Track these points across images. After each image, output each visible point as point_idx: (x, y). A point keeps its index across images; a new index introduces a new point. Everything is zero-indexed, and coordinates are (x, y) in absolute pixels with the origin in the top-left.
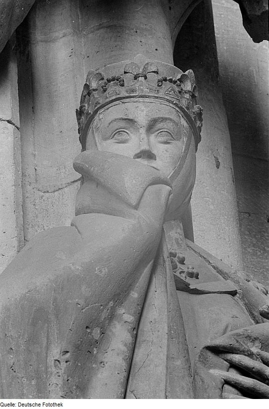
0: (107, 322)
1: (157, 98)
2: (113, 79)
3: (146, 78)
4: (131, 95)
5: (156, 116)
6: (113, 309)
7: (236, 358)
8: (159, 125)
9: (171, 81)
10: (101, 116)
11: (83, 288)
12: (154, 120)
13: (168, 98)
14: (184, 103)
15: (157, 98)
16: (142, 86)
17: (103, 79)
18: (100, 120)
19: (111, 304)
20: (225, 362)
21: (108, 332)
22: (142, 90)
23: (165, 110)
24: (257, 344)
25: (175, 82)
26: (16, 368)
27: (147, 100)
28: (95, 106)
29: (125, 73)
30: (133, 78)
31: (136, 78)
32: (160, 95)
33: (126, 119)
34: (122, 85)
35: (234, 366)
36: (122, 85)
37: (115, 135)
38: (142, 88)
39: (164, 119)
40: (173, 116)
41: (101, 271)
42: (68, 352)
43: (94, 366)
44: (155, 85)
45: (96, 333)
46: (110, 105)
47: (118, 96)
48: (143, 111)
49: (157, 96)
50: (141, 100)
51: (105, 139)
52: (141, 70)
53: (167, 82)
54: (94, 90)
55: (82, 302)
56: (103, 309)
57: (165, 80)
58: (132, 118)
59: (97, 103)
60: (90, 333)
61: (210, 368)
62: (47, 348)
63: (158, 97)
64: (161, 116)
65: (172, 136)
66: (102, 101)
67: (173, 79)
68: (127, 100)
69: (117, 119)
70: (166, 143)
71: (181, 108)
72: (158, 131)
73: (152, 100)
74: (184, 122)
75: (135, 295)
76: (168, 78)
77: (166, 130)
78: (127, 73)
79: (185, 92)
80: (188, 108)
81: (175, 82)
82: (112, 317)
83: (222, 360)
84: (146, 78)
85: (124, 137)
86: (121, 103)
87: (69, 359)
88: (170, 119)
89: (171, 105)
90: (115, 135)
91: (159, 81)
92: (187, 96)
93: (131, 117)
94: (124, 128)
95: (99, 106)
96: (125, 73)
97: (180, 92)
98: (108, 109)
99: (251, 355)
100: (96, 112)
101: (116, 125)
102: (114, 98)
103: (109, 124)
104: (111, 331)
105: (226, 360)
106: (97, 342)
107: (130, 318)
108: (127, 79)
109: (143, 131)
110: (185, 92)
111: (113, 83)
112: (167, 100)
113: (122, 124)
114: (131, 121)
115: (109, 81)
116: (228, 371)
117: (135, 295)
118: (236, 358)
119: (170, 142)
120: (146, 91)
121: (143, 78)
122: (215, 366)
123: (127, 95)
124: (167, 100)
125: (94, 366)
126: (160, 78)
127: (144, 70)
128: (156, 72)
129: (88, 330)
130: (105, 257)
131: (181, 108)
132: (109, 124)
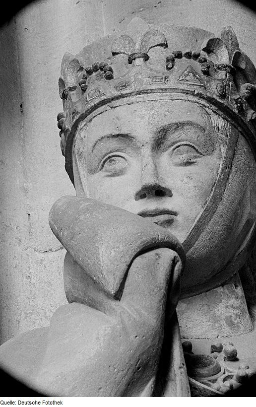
2: (96, 69)
3: (146, 58)
4: (124, 92)
5: (165, 123)
8: (172, 137)
9: (189, 55)
10: (83, 134)
12: (164, 129)
13: (185, 87)
14: (214, 90)
18: (82, 139)
22: (141, 82)
25: (196, 57)
28: (73, 117)
29: (114, 54)
30: (127, 61)
32: (171, 84)
33: (117, 136)
34: (110, 77)
36: (110, 77)
39: (179, 126)
46: (93, 114)
47: (104, 98)
48: (143, 118)
50: (140, 98)
52: (137, 47)
53: (184, 58)
54: (71, 89)
57: (179, 56)
58: (126, 133)
63: (166, 90)
64: (174, 121)
66: (81, 109)
67: (193, 53)
69: (105, 137)
71: (210, 100)
73: (157, 95)
74: (219, 121)
76: (183, 53)
77: (185, 143)
78: (117, 53)
79: (219, 68)
81: (196, 57)
84: (146, 58)
88: (190, 124)
89: (191, 98)
91: (168, 61)
92: (222, 74)
95: (77, 117)
96: (114, 54)
97: (207, 73)
98: (90, 121)
100: (75, 126)
108: (118, 65)
110: (219, 68)
111: (96, 76)
112: (184, 92)
113: (114, 144)
114: (125, 137)
115: (89, 72)
119: (192, 161)
120: (146, 83)
123: (117, 93)
124: (184, 92)
127: (143, 45)
131: (210, 100)
132: (94, 147)
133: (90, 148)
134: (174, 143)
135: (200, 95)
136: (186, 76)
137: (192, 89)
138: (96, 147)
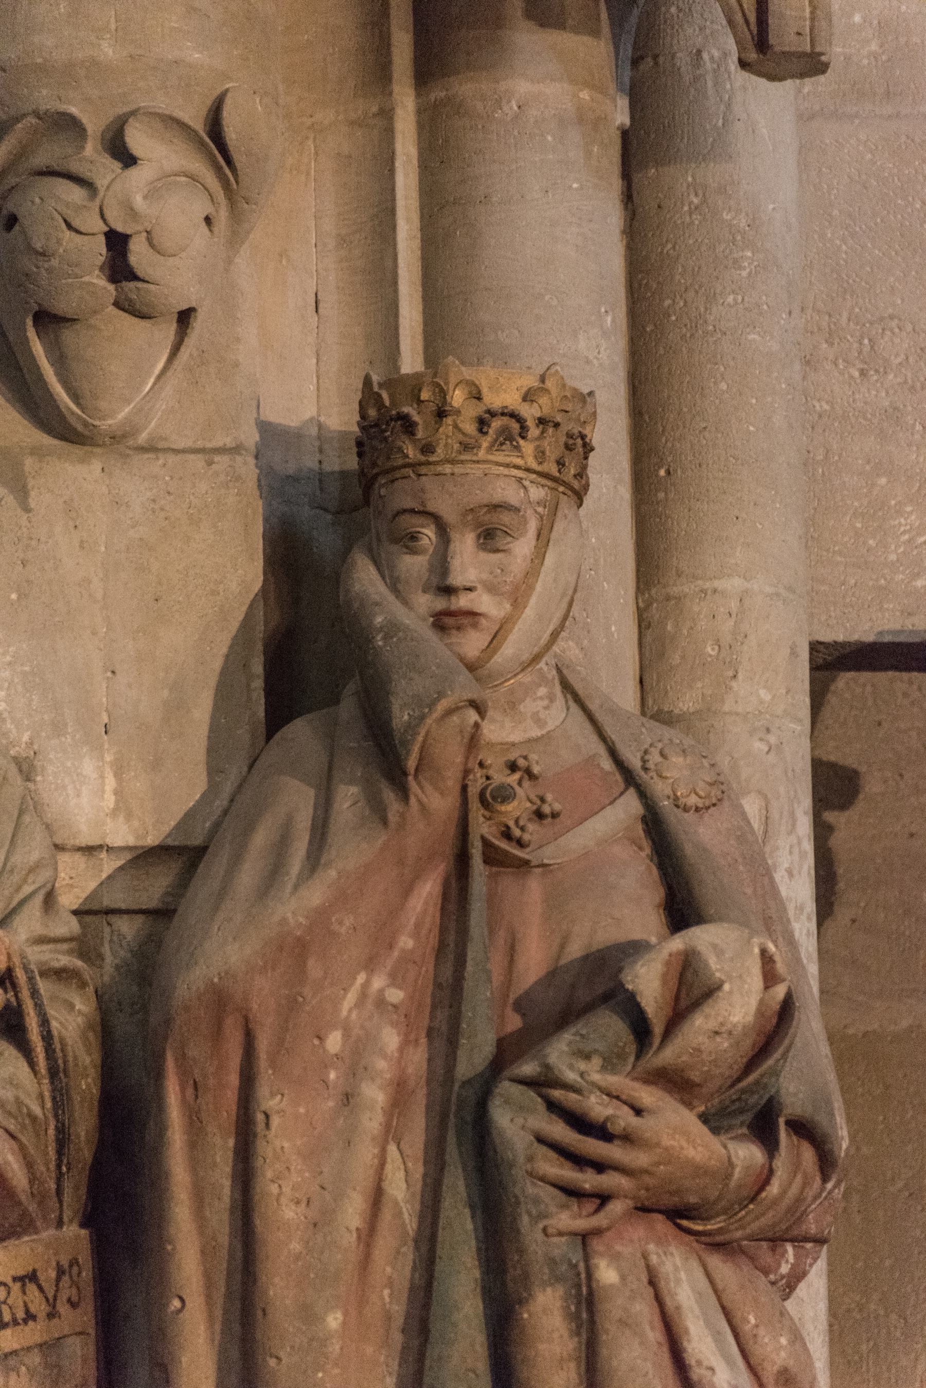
1: (478, 462)
15: (478, 462)
27: (458, 469)
44: (470, 428)
50: (448, 469)
68: (423, 470)
86: (412, 475)
93: (431, 507)
94: (423, 526)
113: (416, 520)
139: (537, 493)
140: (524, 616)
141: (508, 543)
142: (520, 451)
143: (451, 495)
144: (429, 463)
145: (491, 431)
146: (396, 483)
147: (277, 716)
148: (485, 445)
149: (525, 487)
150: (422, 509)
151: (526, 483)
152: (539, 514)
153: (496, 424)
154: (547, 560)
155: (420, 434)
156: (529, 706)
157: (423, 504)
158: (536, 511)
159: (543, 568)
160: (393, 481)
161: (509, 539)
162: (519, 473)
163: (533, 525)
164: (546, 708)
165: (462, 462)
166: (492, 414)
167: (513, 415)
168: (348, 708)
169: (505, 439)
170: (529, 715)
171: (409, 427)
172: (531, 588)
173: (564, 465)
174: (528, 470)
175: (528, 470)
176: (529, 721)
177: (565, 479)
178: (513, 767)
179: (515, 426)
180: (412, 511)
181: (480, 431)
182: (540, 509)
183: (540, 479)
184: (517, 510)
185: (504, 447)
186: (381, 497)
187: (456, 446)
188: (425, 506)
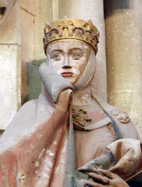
0: (42, 158)
1: (72, 38)
4: (61, 38)
6: (45, 151)
7: (91, 174)
9: (79, 28)
11: (31, 145)
13: (77, 38)
15: (72, 38)
16: (65, 33)
17: (50, 28)
19: (44, 150)
20: (87, 175)
21: (43, 162)
22: (66, 35)
23: (77, 44)
24: (101, 166)
26: (5, 182)
27: (67, 40)
29: (59, 26)
31: (63, 28)
32: (73, 37)
34: (57, 33)
35: (90, 177)
37: (55, 57)
38: (65, 34)
39: (76, 49)
40: (80, 47)
41: (39, 136)
42: (24, 175)
43: (36, 179)
44: (71, 31)
45: (37, 164)
47: (55, 39)
48: (66, 46)
49: (72, 38)
50: (65, 40)
51: (52, 58)
55: (31, 152)
56: (40, 152)
59: (48, 41)
60: (34, 165)
61: (81, 178)
62: (17, 173)
64: (74, 47)
65: (79, 56)
68: (59, 41)
70: (77, 59)
72: (73, 54)
73: (70, 40)
75: (55, 143)
80: (87, 40)
82: (44, 155)
83: (86, 175)
85: (59, 58)
87: (25, 178)
89: (79, 41)
90: (55, 57)
93: (61, 49)
94: (59, 54)
96: (59, 26)
99: (96, 173)
101: (55, 53)
102: (54, 39)
103: (52, 52)
104: (44, 161)
105: (88, 175)
106: (37, 168)
107: (52, 154)
108: (60, 29)
109: (66, 55)
112: (77, 39)
113: (57, 52)
114: (61, 51)
116: (88, 180)
117: (55, 143)
118: (91, 174)
120: (67, 36)
121: (66, 29)
122: (83, 178)
123: (59, 38)
124: (77, 39)
125: (36, 179)
126: (74, 28)
128: (72, 25)
129: (33, 164)
130: (41, 129)
133: (51, 52)
134: (74, 53)
135: (81, 40)
136: (78, 35)
137: (79, 38)
138: (53, 52)
139: (86, 47)
140: (83, 75)
141: (79, 57)
142: (82, 36)
143: (66, 46)
144: (60, 39)
145: (75, 32)
146: (53, 45)
147: (25, 100)
148: (74, 35)
149: (83, 45)
150: (59, 49)
151: (84, 44)
152: (86, 52)
153: (76, 30)
154: (88, 63)
155: (60, 33)
156: (84, 98)
157: (59, 48)
158: (86, 51)
159: (87, 65)
160: (52, 44)
161: (79, 57)
162: (82, 42)
163: (85, 54)
164: (88, 99)
165: (68, 38)
166: (76, 28)
167: (81, 29)
168: (42, 96)
169: (79, 34)
170: (84, 100)
171: (57, 32)
172: (84, 68)
173: (92, 42)
174: (84, 41)
175: (84, 41)
176: (84, 101)
177: (92, 45)
178: (80, 110)
179: (81, 31)
180: (57, 50)
181: (73, 32)
182: (87, 51)
183: (87, 44)
184: (81, 50)
185: (78, 35)
186: (49, 49)
187: (67, 35)
188: (59, 49)
